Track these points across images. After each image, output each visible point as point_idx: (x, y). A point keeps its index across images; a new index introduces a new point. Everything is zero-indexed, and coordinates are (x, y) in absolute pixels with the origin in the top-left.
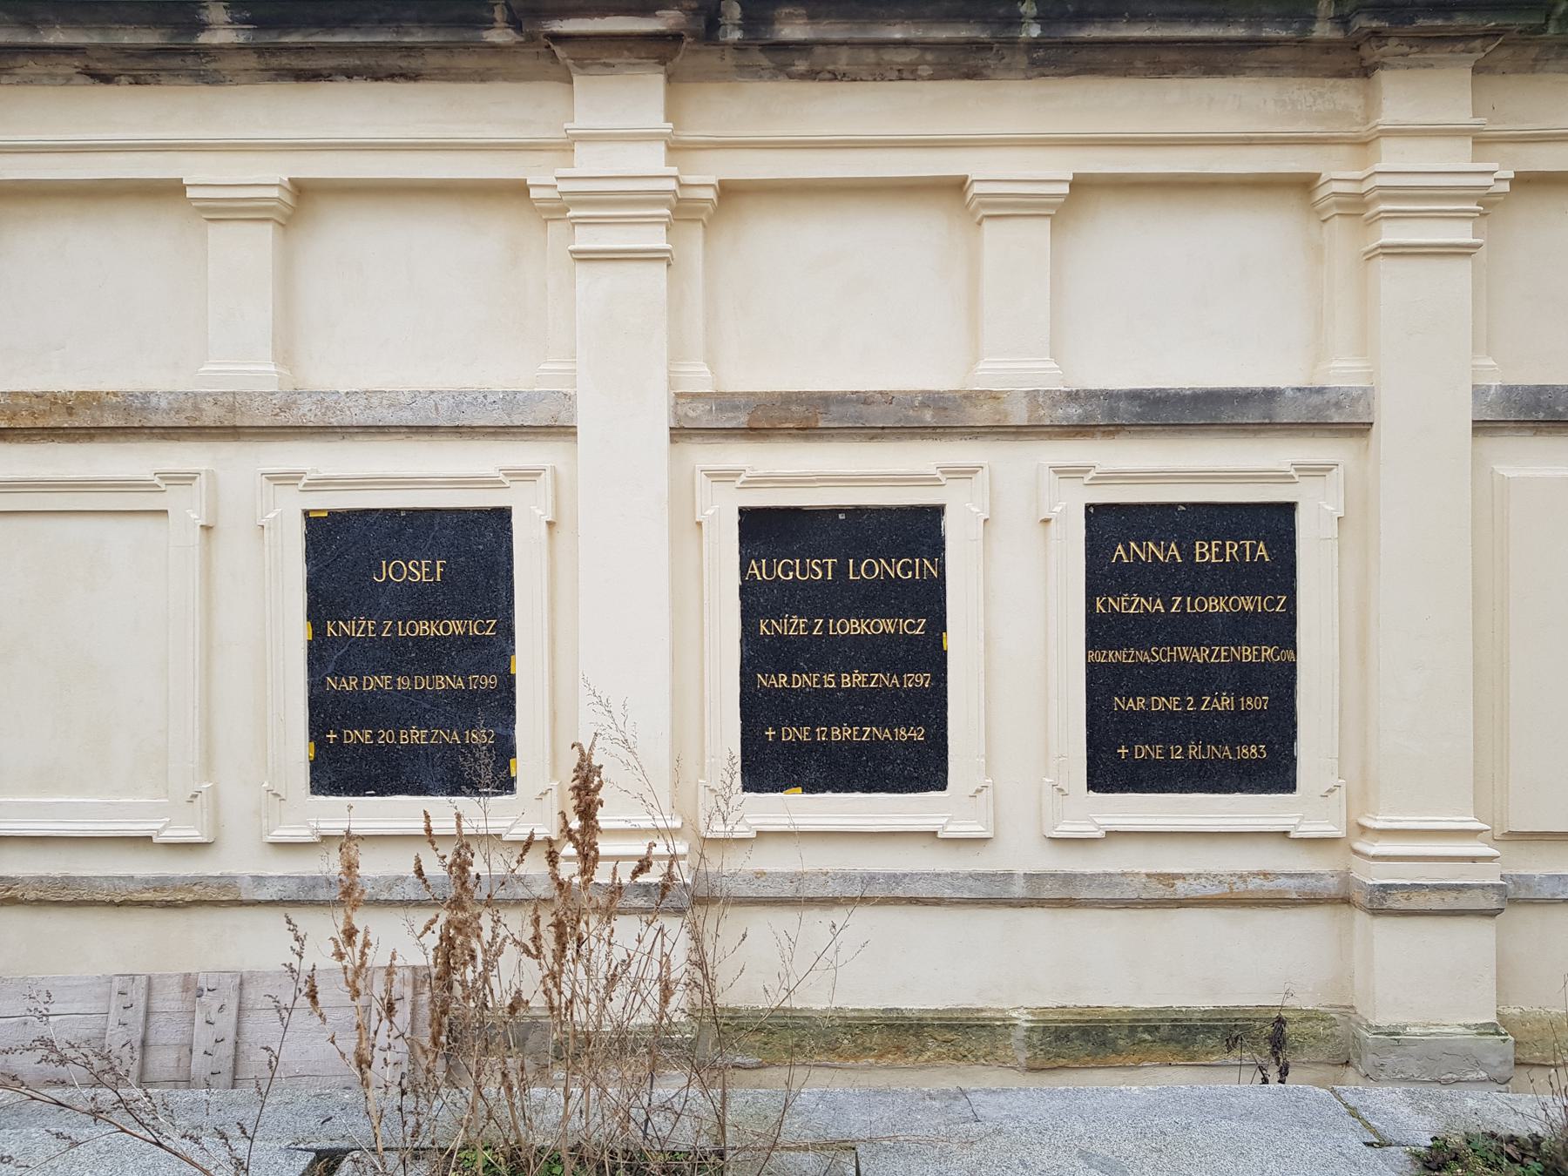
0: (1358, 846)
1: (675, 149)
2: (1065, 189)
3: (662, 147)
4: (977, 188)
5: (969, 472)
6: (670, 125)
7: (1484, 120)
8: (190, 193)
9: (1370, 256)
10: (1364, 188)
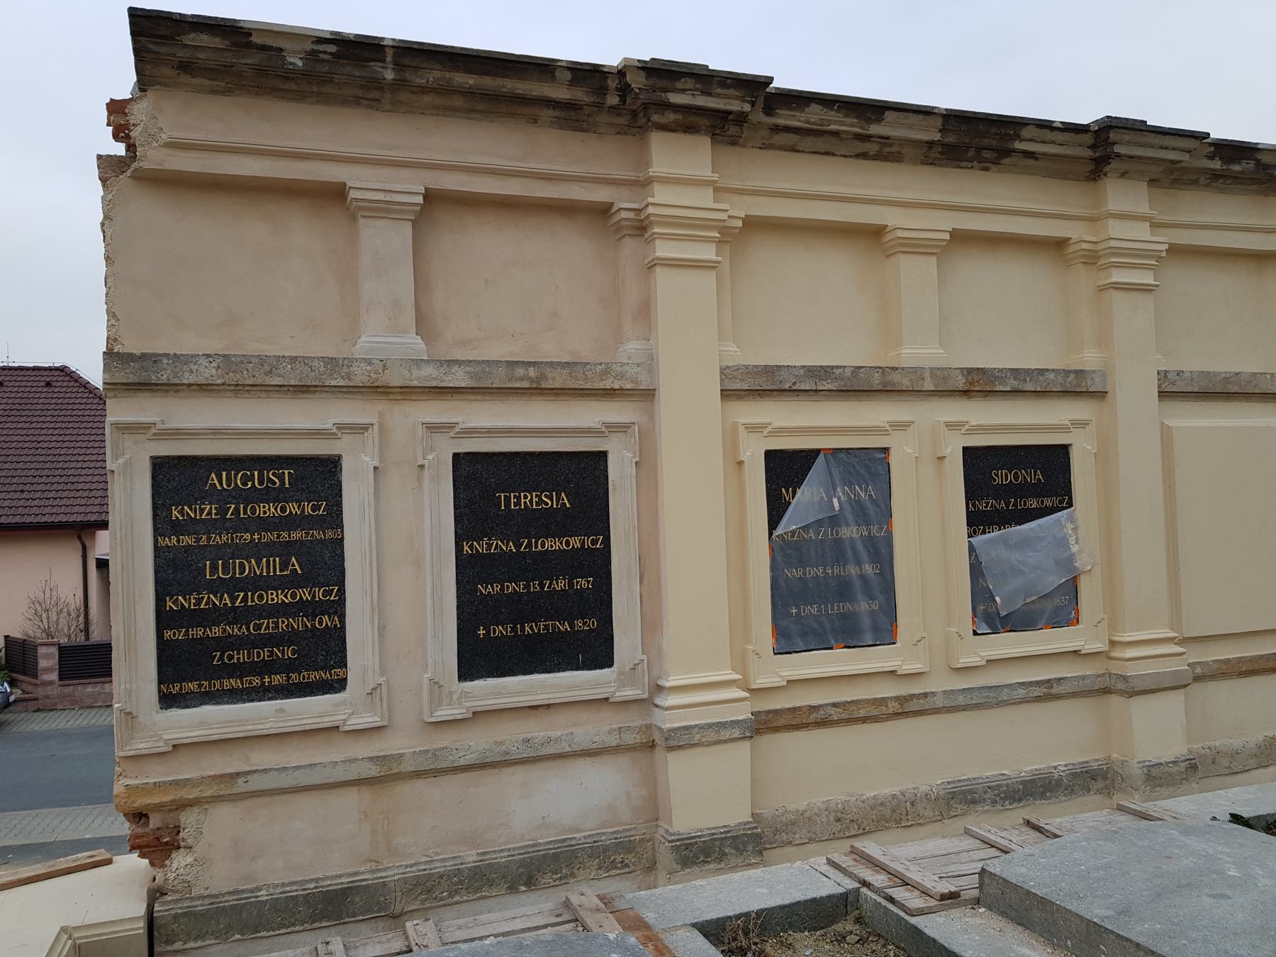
0: (1114, 654)
1: (717, 190)
2: (947, 237)
4: (900, 234)
9: (1103, 289)
10: (1098, 247)
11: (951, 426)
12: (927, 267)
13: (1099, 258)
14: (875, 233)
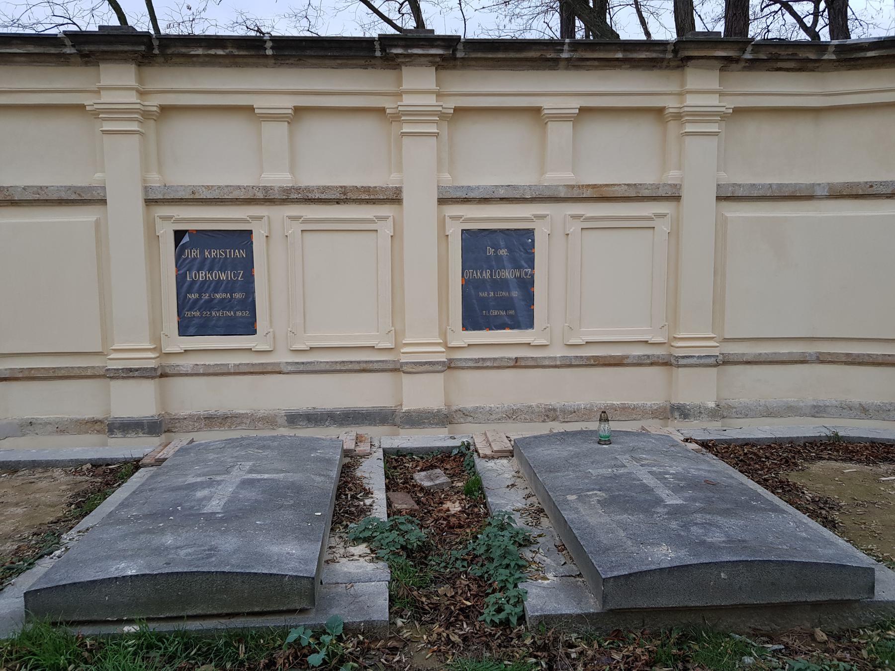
0: (672, 344)
2: (577, 111)
3: (434, 96)
4: (546, 111)
5: (543, 217)
6: (438, 88)
7: (722, 88)
8: (257, 111)
10: (682, 111)
11: (574, 217)
12: (567, 128)
13: (682, 117)
14: (537, 110)
